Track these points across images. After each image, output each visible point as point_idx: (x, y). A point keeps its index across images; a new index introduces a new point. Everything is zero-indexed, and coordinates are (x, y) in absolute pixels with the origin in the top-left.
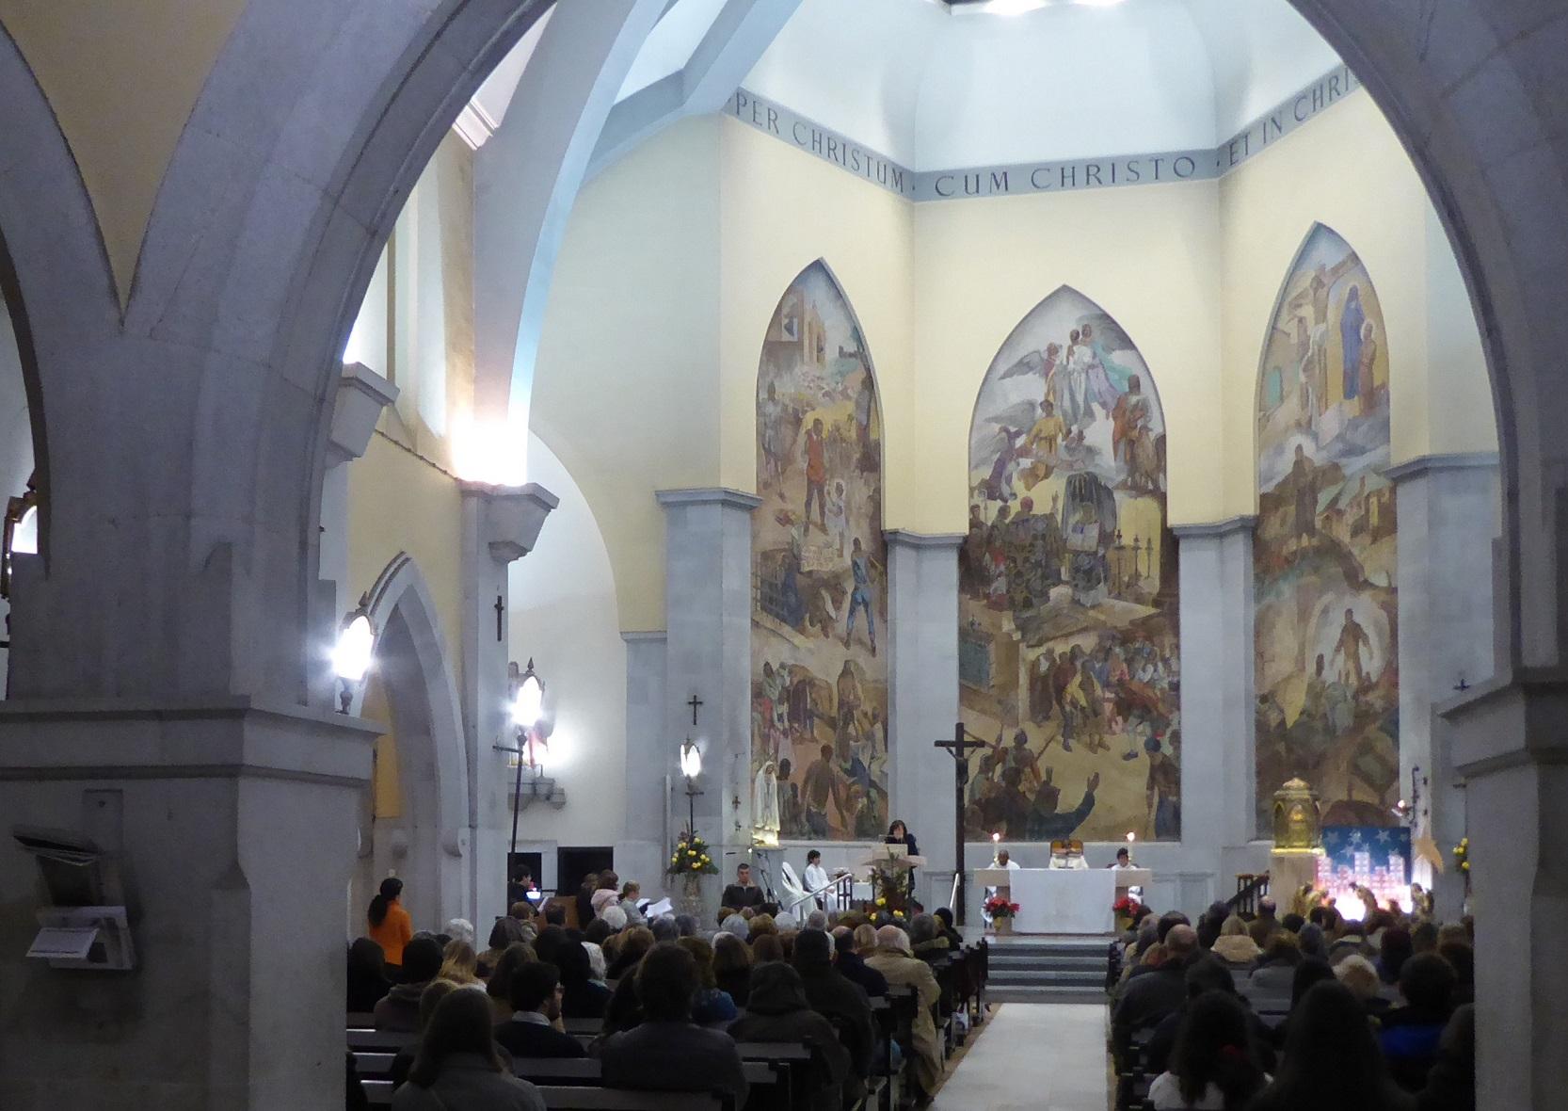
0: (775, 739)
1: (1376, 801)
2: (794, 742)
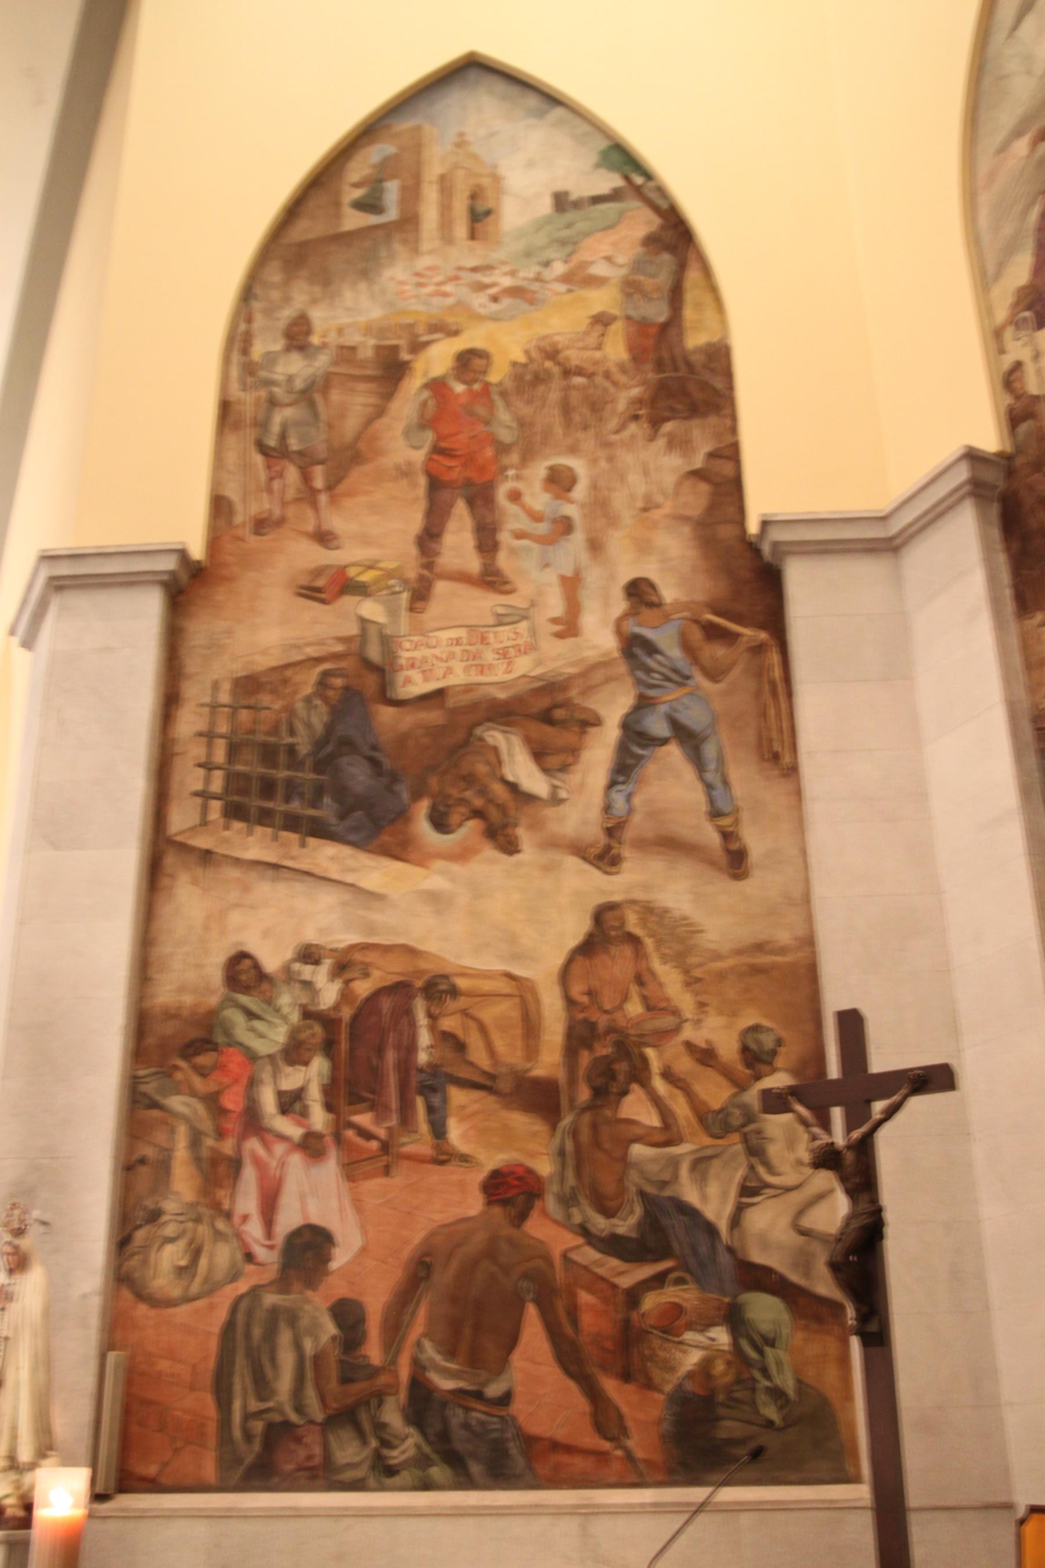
0: (258, 1163)
2: (351, 1171)
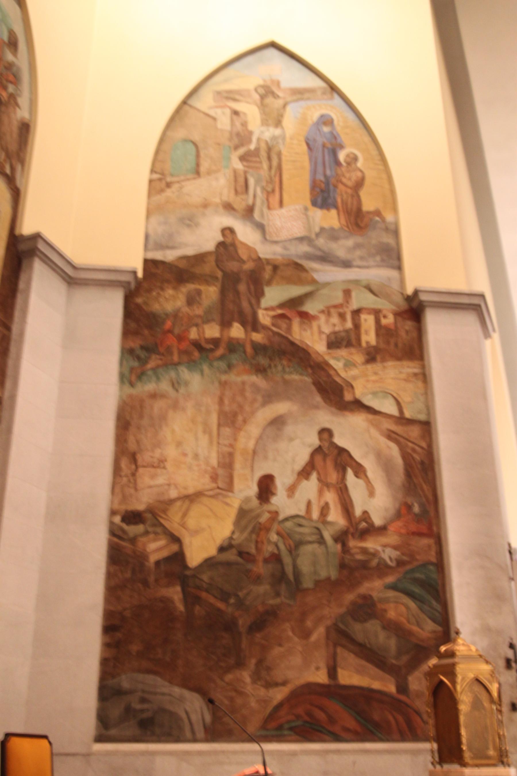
1: (392, 688)
